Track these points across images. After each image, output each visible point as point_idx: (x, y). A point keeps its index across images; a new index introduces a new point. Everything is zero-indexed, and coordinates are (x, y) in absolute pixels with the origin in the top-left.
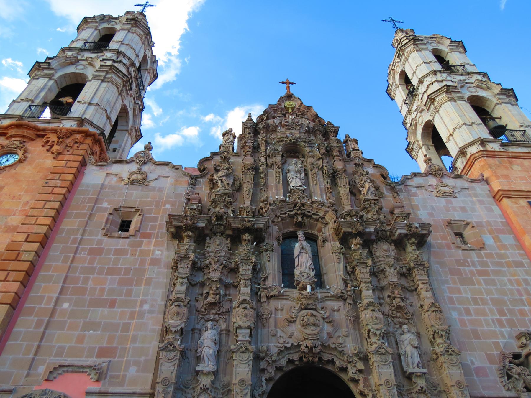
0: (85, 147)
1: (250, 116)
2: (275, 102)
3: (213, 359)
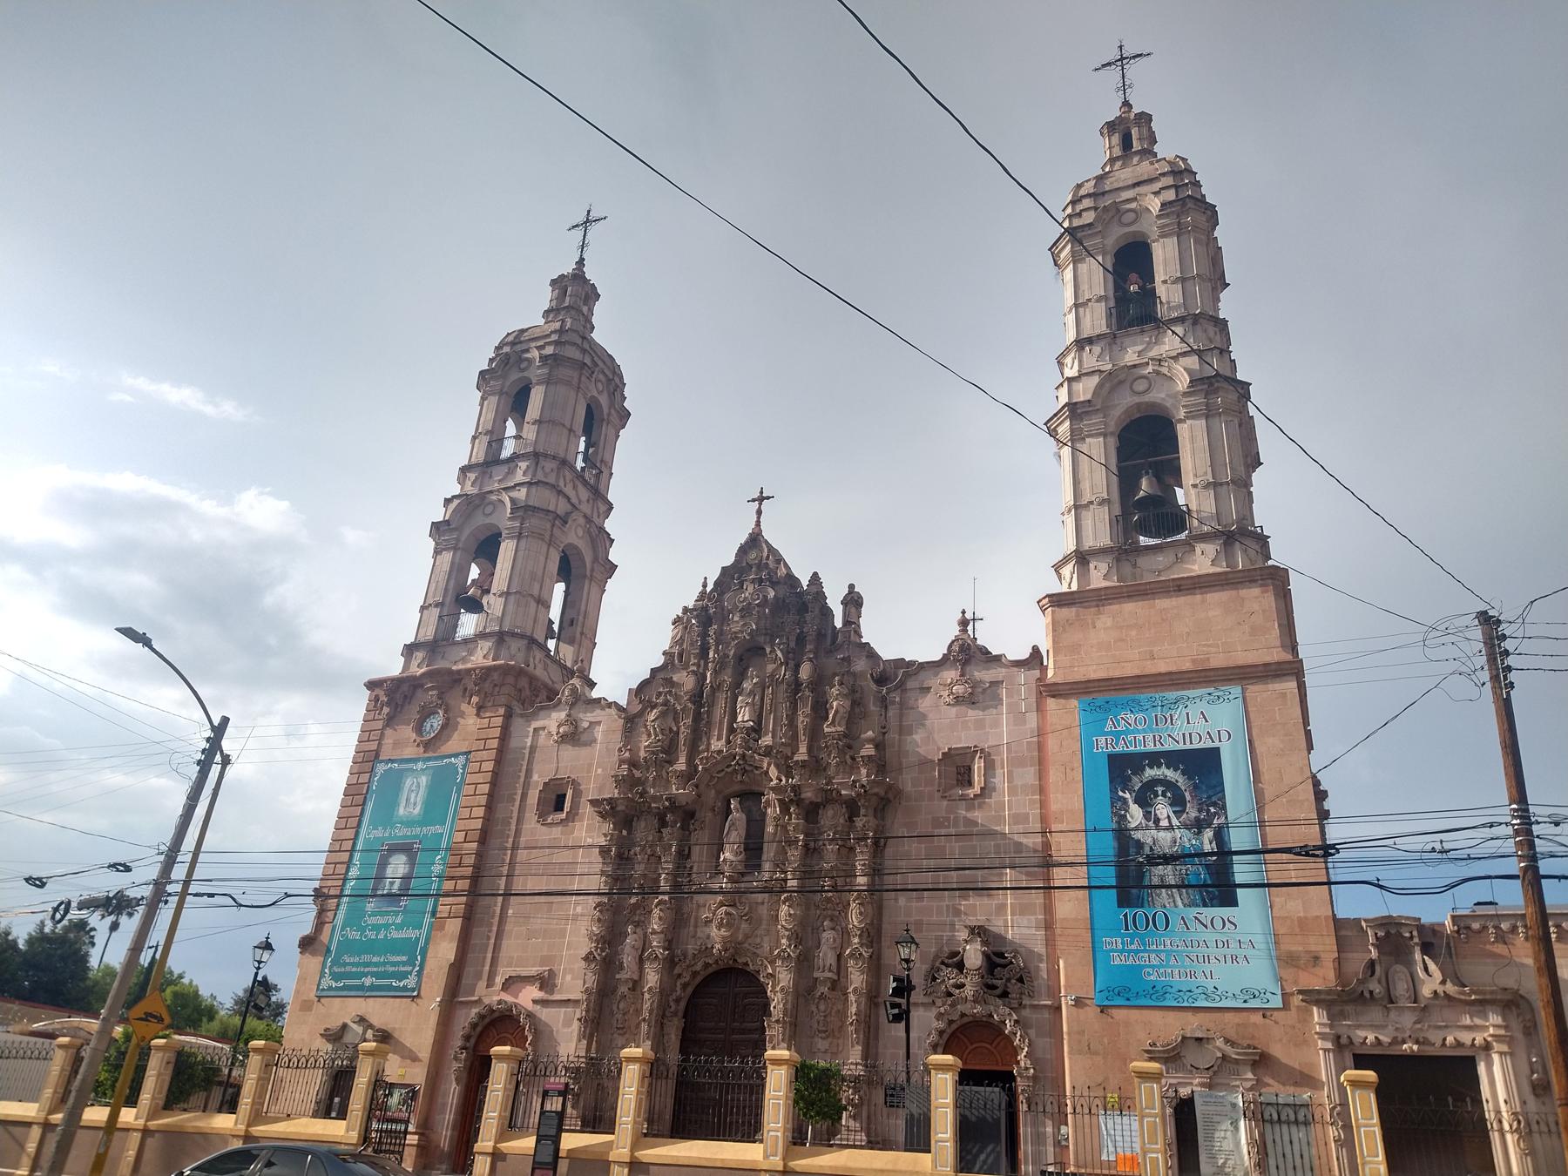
0: (505, 690)
1: (705, 586)
2: (729, 560)
3: (635, 967)
